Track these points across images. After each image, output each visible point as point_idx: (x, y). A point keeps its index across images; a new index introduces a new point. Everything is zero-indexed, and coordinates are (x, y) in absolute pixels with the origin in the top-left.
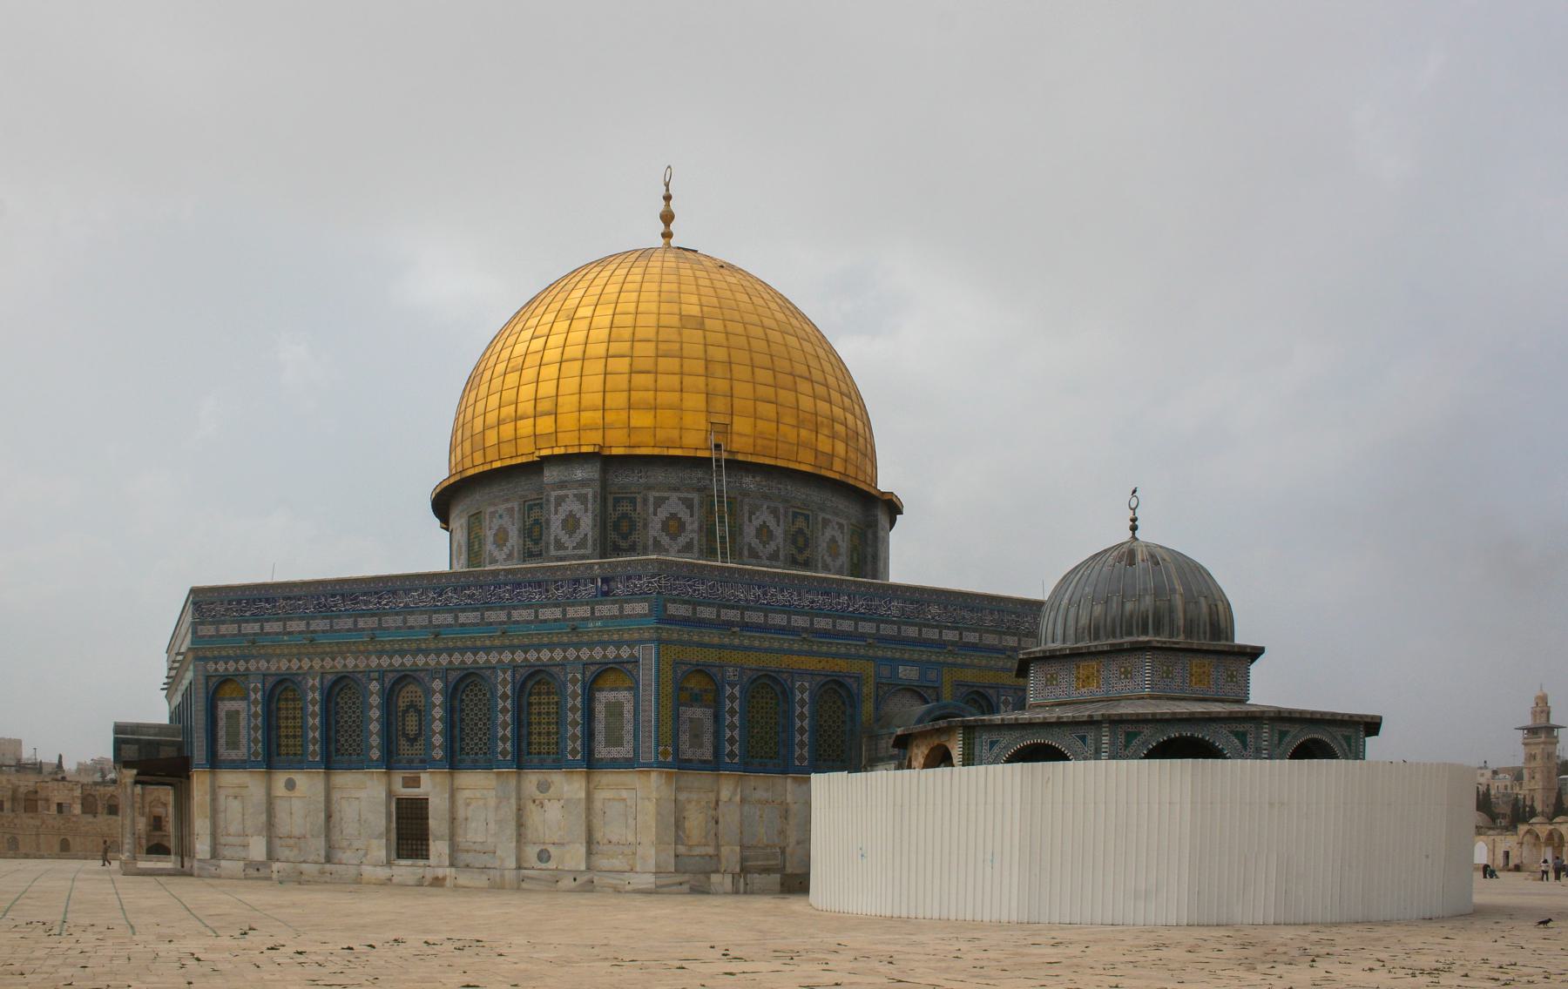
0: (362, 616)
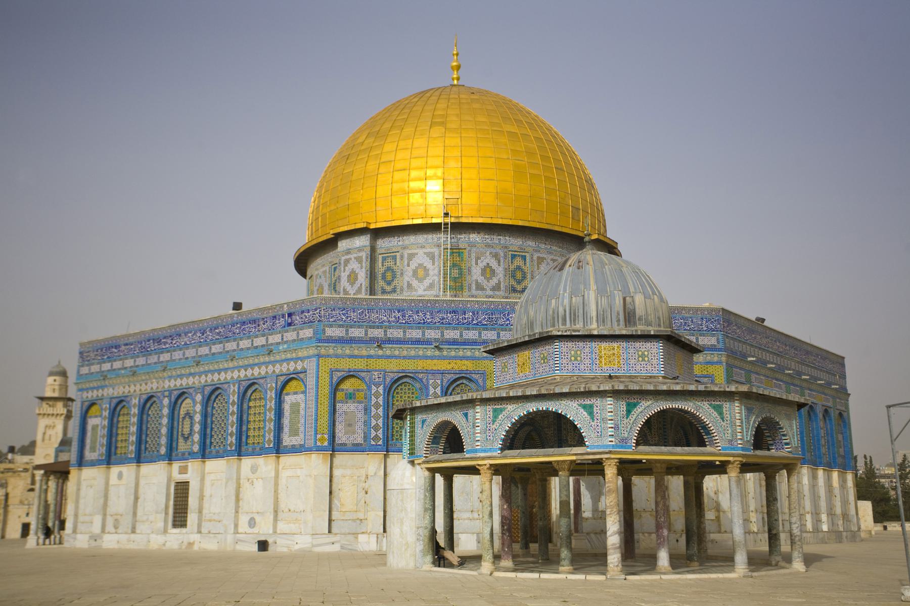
0: (162, 353)
